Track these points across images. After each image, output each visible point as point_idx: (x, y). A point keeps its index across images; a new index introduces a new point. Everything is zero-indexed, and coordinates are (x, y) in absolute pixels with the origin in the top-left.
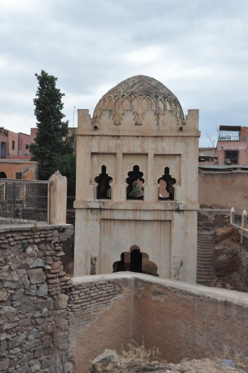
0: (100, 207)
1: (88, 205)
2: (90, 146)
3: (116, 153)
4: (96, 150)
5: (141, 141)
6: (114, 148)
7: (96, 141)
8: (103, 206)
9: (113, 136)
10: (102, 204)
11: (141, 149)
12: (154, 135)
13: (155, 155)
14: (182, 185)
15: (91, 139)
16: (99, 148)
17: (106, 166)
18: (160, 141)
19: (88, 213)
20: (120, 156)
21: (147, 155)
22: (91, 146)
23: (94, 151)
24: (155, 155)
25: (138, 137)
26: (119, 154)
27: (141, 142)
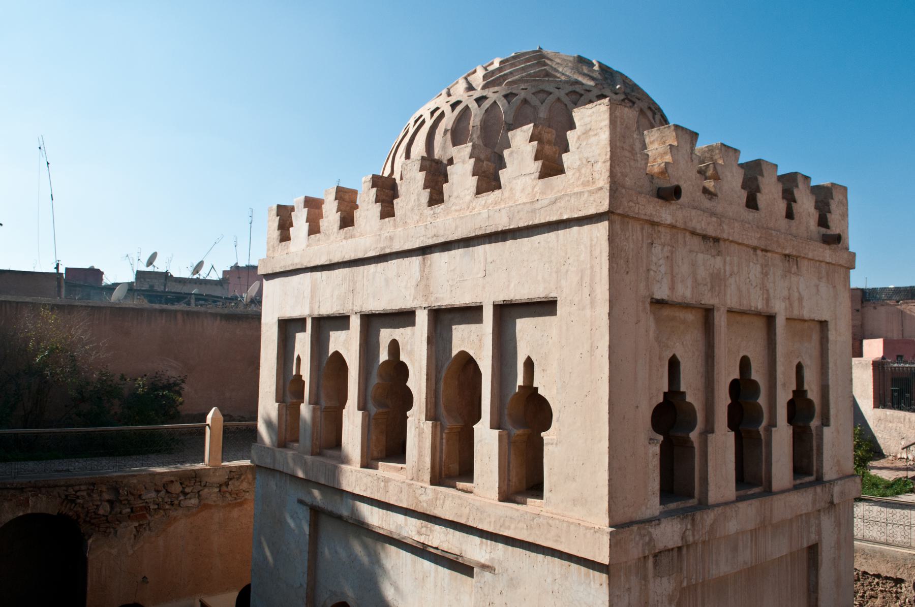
0: (682, 539)
1: (651, 539)
3: (713, 306)
4: (662, 292)
6: (709, 285)
7: (662, 250)
8: (691, 532)
9: (705, 237)
10: (689, 527)
11: (763, 299)
12: (787, 252)
13: (787, 319)
15: (650, 241)
16: (672, 288)
18: (795, 273)
19: (645, 578)
20: (721, 320)
21: (770, 319)
22: (652, 273)
23: (658, 296)
24: (787, 319)
25: (755, 249)
26: (719, 310)
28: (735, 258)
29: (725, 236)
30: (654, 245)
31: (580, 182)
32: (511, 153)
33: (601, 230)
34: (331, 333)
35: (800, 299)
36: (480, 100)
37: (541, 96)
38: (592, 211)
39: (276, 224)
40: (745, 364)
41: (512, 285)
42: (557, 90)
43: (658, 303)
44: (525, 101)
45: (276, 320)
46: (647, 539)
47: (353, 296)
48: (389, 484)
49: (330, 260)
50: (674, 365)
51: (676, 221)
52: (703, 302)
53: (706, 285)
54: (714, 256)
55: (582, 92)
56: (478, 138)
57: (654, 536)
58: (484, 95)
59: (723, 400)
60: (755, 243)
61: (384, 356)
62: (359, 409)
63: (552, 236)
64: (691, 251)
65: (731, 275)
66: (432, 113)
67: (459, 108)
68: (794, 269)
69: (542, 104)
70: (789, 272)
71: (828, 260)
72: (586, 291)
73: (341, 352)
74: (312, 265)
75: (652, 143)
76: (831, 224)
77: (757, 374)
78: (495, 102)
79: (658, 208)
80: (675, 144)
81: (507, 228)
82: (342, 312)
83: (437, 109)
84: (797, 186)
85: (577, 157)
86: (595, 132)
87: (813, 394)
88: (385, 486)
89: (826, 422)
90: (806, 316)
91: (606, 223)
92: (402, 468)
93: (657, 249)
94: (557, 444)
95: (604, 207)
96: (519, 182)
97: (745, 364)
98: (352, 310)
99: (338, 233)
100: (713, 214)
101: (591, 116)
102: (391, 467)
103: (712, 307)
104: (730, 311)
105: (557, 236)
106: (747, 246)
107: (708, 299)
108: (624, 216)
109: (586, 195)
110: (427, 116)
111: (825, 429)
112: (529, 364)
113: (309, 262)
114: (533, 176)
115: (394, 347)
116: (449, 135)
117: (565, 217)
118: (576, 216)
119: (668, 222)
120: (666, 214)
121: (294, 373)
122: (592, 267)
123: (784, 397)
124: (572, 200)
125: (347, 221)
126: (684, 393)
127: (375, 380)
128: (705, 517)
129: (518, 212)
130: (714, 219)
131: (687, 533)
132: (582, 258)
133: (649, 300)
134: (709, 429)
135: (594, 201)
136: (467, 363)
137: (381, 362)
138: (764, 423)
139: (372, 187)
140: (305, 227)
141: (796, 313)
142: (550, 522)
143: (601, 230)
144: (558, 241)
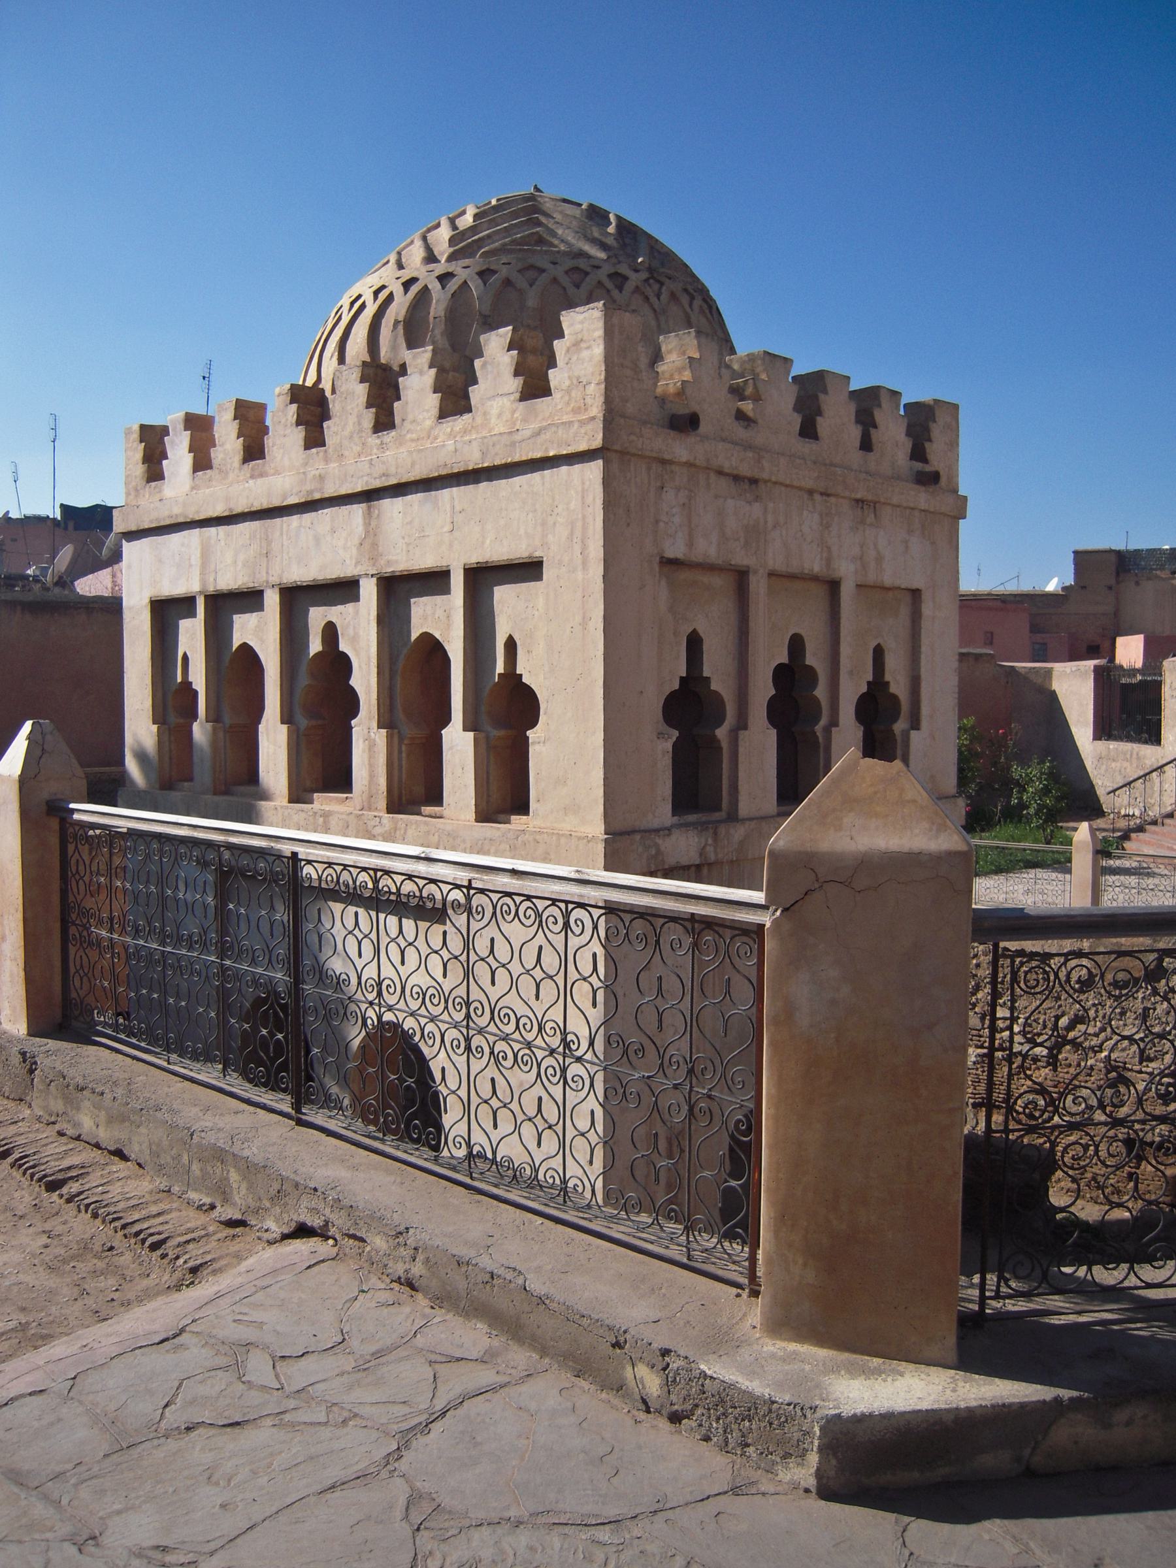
1: (659, 852)
2: (657, 522)
3: (748, 567)
4: (676, 549)
5: (821, 515)
6: (742, 540)
8: (712, 849)
9: (737, 478)
10: (710, 841)
11: (821, 559)
12: (859, 496)
13: (857, 586)
14: (924, 723)
15: (659, 484)
16: (690, 544)
17: (702, 635)
18: (871, 525)
20: (758, 585)
21: (834, 586)
22: (662, 525)
23: (670, 554)
24: (857, 586)
25: (811, 492)
26: (756, 572)
27: (821, 524)
28: (781, 505)
29: (765, 476)
30: (665, 489)
31: (569, 409)
32: (484, 365)
33: (594, 471)
34: (236, 617)
35: (879, 559)
36: (444, 278)
37: (531, 274)
38: (583, 447)
39: (139, 455)
40: (796, 645)
41: (488, 542)
42: (552, 266)
43: (671, 564)
44: (508, 282)
45: (148, 600)
46: (653, 852)
47: (268, 561)
48: (331, 818)
49: (230, 510)
50: (694, 644)
51: (695, 459)
52: (733, 563)
53: (738, 540)
54: (750, 503)
55: (588, 269)
56: (442, 334)
57: (662, 848)
58: (450, 270)
59: (763, 689)
60: (809, 484)
61: (315, 646)
62: (283, 722)
63: (536, 477)
64: (716, 497)
65: (775, 527)
66: (376, 293)
67: (415, 289)
68: (871, 518)
69: (531, 285)
70: (863, 522)
71: (923, 506)
72: (577, 549)
73: (251, 644)
74: (202, 517)
75: (670, 352)
76: (931, 457)
77: (814, 658)
78: (465, 282)
79: (670, 441)
80: (697, 356)
81: (480, 466)
82: (251, 585)
83: (383, 287)
84: (880, 406)
85: (566, 375)
86: (588, 344)
87: (898, 686)
88: (325, 822)
89: (915, 724)
90: (888, 581)
91: (600, 462)
92: (347, 798)
93: (669, 496)
94: (544, 742)
95: (597, 442)
96: (494, 403)
97: (796, 645)
98: (267, 582)
99: (240, 469)
100: (748, 447)
101: (582, 322)
102: (331, 799)
103: (744, 569)
104: (772, 574)
105: (543, 477)
106: (800, 488)
107: (741, 559)
108: (623, 453)
109: (576, 425)
110: (368, 297)
111: (913, 733)
112: (511, 645)
113: (198, 512)
114: (512, 397)
115: (330, 632)
116: (400, 328)
117: (551, 454)
118: (565, 452)
119: (684, 459)
120: (681, 449)
121: (179, 680)
122: (584, 517)
123: (851, 690)
124: (560, 432)
125: (254, 451)
126: (708, 679)
127: (304, 680)
128: (732, 831)
129: (494, 445)
130: (750, 454)
131: (708, 848)
132: (572, 506)
133: (658, 559)
134: (742, 724)
135: (586, 434)
136: (433, 649)
137: (311, 654)
138: (823, 722)
139: (291, 403)
140: (187, 460)
141: (871, 578)
142: (538, 837)
143: (594, 471)
144: (543, 484)
